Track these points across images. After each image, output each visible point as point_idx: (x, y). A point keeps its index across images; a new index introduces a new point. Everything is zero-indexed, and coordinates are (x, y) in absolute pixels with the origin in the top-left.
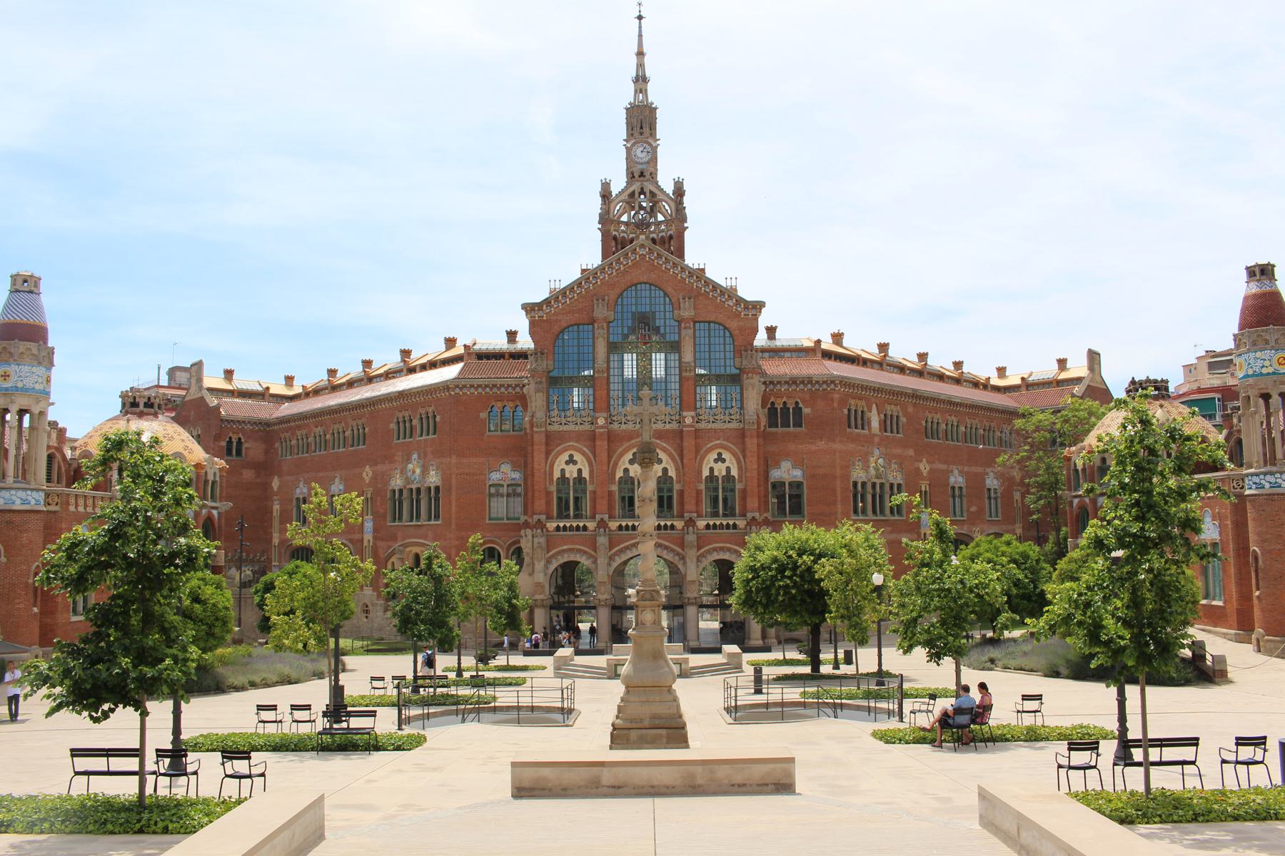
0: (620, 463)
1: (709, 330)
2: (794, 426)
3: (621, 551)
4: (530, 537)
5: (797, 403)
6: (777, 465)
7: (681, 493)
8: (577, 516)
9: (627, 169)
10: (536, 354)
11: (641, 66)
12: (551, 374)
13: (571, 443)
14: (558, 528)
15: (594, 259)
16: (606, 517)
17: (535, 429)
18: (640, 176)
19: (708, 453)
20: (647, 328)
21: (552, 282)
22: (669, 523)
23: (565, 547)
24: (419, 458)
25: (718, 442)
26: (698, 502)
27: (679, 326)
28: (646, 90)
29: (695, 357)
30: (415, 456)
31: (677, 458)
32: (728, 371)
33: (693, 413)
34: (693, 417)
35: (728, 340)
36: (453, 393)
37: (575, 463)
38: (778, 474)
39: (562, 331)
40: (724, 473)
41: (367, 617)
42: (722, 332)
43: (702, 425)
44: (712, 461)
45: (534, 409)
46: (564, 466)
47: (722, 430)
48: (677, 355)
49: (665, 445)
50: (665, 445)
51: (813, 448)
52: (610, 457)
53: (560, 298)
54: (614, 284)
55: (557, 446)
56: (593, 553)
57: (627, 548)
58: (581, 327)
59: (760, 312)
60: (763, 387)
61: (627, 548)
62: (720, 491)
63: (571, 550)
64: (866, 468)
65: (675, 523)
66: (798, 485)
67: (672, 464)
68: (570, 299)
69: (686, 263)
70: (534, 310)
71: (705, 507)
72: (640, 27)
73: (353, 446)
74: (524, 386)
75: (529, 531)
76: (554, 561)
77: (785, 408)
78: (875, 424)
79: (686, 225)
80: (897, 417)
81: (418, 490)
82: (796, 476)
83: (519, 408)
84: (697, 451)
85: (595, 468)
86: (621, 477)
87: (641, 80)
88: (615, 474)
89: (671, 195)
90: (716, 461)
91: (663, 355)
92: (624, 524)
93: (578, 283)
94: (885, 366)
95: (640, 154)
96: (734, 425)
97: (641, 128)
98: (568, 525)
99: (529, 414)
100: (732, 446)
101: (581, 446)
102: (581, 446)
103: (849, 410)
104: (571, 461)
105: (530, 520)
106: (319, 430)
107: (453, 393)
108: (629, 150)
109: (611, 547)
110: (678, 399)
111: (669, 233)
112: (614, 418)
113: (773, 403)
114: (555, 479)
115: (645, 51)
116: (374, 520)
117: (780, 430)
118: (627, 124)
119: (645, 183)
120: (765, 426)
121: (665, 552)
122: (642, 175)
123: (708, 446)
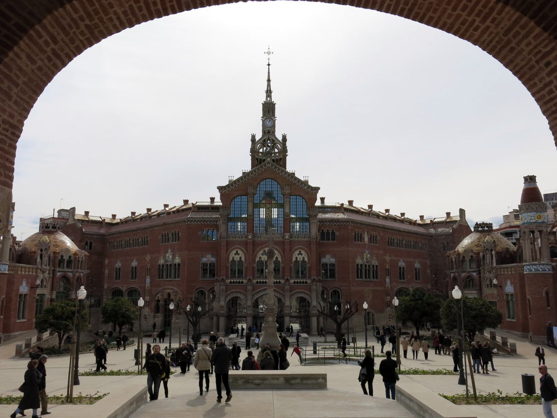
0: (258, 255)
1: (296, 199)
2: (332, 240)
4: (219, 286)
5: (333, 230)
6: (324, 257)
7: (283, 268)
8: (239, 277)
9: (262, 130)
10: (223, 208)
11: (269, 85)
12: (229, 216)
13: (237, 246)
14: (231, 282)
15: (248, 167)
16: (251, 278)
17: (222, 240)
18: (268, 133)
21: (230, 177)
23: (234, 291)
24: (171, 251)
25: (299, 246)
26: (291, 272)
27: (284, 197)
28: (271, 96)
29: (290, 210)
30: (170, 250)
31: (282, 253)
32: (304, 216)
33: (289, 234)
34: (289, 236)
35: (304, 203)
36: (187, 224)
37: (239, 254)
38: (324, 260)
39: (234, 198)
40: (302, 260)
41: (146, 321)
42: (302, 200)
43: (293, 239)
44: (297, 254)
45: (221, 231)
46: (234, 256)
48: (282, 209)
49: (277, 247)
50: (277, 247)
52: (253, 252)
53: (234, 184)
55: (232, 247)
56: (245, 293)
57: (260, 291)
58: (242, 197)
59: (318, 192)
60: (319, 223)
61: (260, 291)
62: (300, 267)
63: (236, 292)
64: (362, 258)
65: (281, 281)
66: (333, 265)
68: (238, 185)
69: (287, 170)
70: (222, 189)
71: (293, 274)
72: (269, 69)
73: (142, 246)
74: (217, 221)
75: (218, 283)
77: (328, 232)
78: (366, 239)
79: (287, 154)
80: (376, 237)
81: (171, 265)
82: (332, 261)
83: (215, 231)
84: (290, 250)
85: (247, 256)
86: (258, 261)
87: (269, 92)
89: (281, 141)
90: (298, 254)
91: (276, 209)
92: (259, 281)
93: (241, 178)
94: (371, 215)
95: (269, 123)
96: (306, 239)
97: (269, 112)
98: (235, 281)
99: (219, 233)
100: (306, 249)
101: (241, 247)
102: (241, 247)
103: (355, 233)
104: (237, 253)
105: (219, 279)
106: (127, 238)
107: (187, 224)
108: (263, 122)
109: (253, 290)
110: (283, 228)
111: (280, 157)
112: (256, 236)
113: (323, 230)
114: (230, 261)
115: (271, 79)
116: (151, 278)
117: (326, 241)
118: (263, 110)
119: (270, 136)
120: (319, 240)
122: (269, 132)
123: (295, 248)
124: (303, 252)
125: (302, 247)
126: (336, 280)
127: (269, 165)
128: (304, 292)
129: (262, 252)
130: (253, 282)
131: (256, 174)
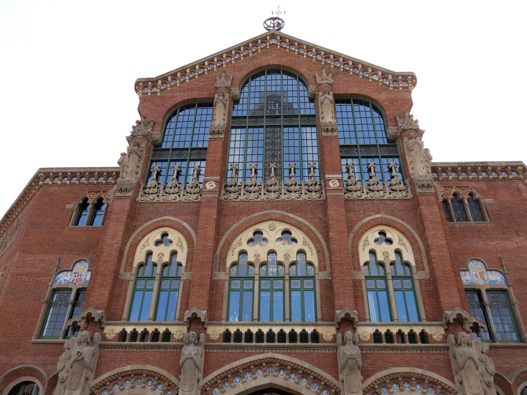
13: (167, 217)
20: (277, 105)
23: (128, 368)
25: (378, 216)
31: (320, 236)
40: (393, 257)
44: (371, 240)
51: (509, 244)
54: (242, 67)
56: (173, 379)
67: (312, 245)
88: (225, 257)
101: (180, 221)
102: (180, 221)
114: (135, 265)
121: (304, 382)
123: (365, 221)
124: (391, 234)
127: (274, 41)
130: (207, 336)
131: (239, 58)
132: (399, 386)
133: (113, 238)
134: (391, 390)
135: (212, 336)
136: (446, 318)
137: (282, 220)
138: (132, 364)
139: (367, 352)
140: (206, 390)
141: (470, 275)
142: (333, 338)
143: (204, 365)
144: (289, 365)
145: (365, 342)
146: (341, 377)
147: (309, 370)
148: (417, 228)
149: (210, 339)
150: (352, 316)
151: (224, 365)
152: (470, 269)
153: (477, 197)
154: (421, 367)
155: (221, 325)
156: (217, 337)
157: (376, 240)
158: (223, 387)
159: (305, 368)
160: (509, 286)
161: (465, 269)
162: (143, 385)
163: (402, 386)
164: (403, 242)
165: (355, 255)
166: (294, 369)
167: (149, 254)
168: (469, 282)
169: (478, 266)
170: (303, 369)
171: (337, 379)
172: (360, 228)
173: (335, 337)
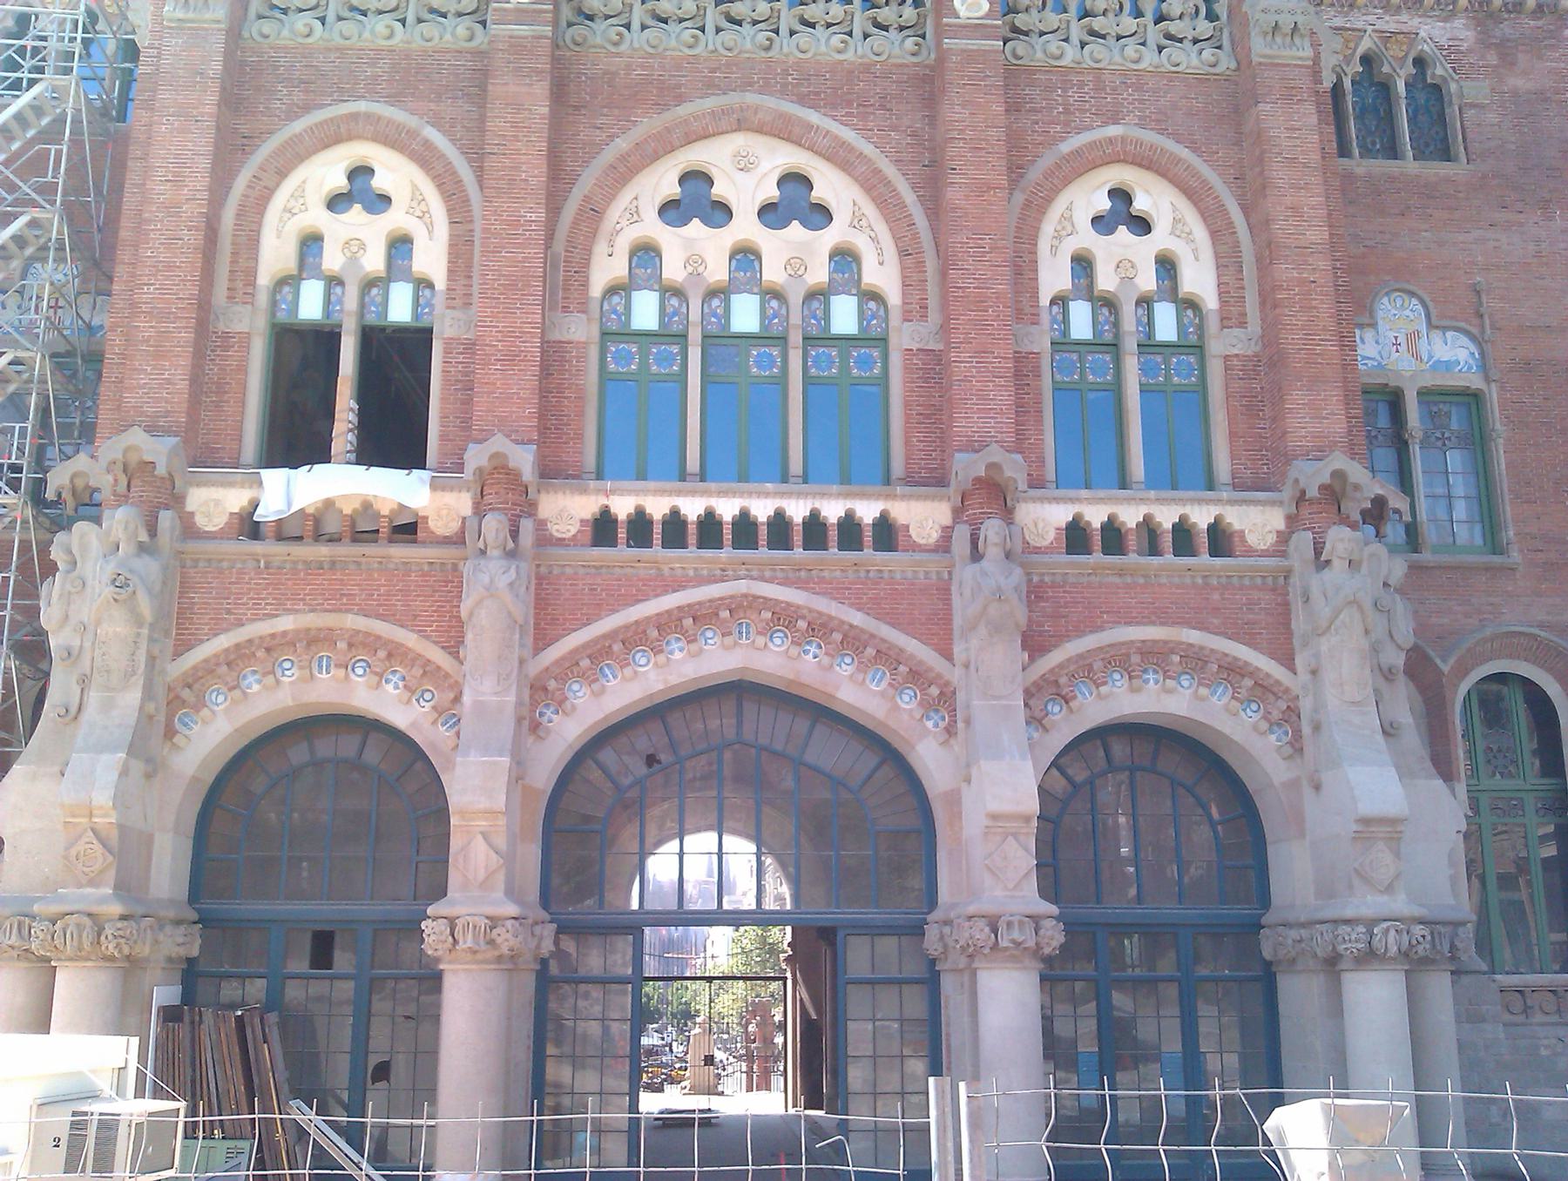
0: (616, 211)
3: (599, 652)
13: (362, 106)
19: (1067, 182)
22: (868, 511)
23: (286, 623)
31: (909, 197)
40: (1147, 281)
44: (1083, 219)
47: (1135, 80)
49: (848, 135)
50: (848, 135)
57: (635, 639)
67: (882, 229)
76: (219, 700)
82: (1448, 366)
88: (586, 263)
100: (1184, 153)
101: (412, 121)
102: (412, 121)
114: (264, 279)
123: (1066, 147)
124: (1152, 197)
125: (1149, 137)
126: (1515, 556)
128: (1195, 662)
129: (663, 181)
130: (541, 525)
132: (1130, 678)
133: (177, 181)
134: (1103, 689)
135: (556, 527)
136: (1297, 481)
137: (784, 131)
138: (297, 611)
139: (1042, 581)
140: (545, 689)
141: (1377, 342)
142: (942, 537)
143: (536, 613)
144: (803, 617)
145: (1038, 550)
146: (958, 649)
147: (862, 630)
148: (1238, 180)
149: (551, 535)
150: (1008, 473)
151: (599, 618)
152: (1380, 322)
153: (1439, 71)
154: (1201, 626)
155: (584, 491)
156: (573, 531)
157: (1097, 220)
158: (597, 680)
159: (851, 626)
160: (1488, 380)
161: (1366, 320)
162: (342, 672)
163: (1139, 677)
164: (1188, 230)
165: (1024, 270)
166: (819, 628)
167: (311, 243)
168: (1370, 363)
169: (1407, 312)
170: (846, 627)
171: (948, 656)
172: (1049, 174)
173: (947, 534)
